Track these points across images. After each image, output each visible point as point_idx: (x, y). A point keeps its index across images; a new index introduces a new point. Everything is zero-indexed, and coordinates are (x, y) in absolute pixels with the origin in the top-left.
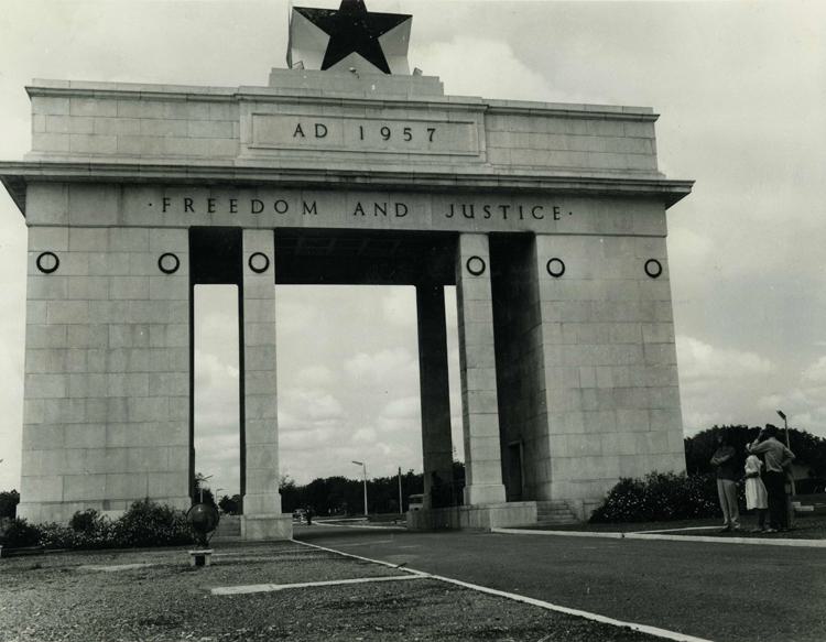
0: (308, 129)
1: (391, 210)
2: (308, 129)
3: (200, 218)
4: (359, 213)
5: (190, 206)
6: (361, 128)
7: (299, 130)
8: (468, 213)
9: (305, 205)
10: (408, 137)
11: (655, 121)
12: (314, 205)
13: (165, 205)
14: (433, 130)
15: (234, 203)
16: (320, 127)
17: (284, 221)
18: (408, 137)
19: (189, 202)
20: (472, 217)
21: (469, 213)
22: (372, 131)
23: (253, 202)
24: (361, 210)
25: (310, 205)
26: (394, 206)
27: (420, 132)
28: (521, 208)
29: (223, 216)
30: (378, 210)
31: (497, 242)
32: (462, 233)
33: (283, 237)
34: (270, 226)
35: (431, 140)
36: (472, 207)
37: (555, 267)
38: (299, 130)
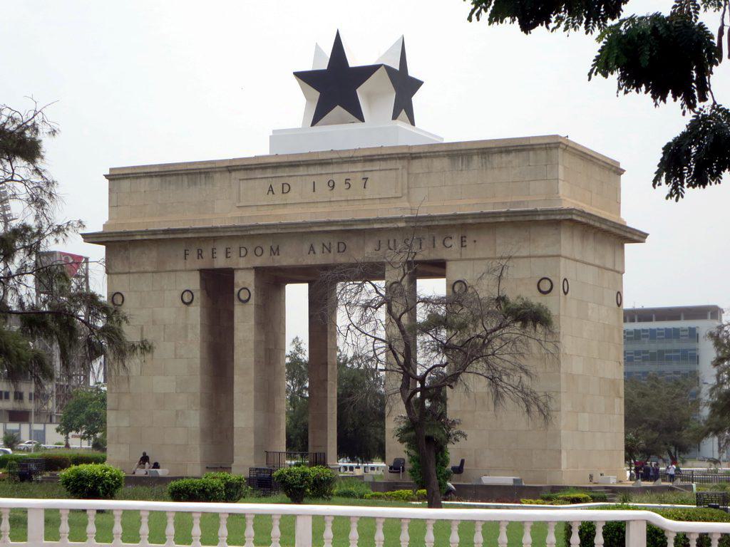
0: (278, 188)
1: (335, 248)
2: (278, 188)
4: (312, 252)
5: (201, 254)
7: (271, 189)
10: (347, 186)
13: (185, 254)
17: (259, 262)
18: (347, 186)
19: (200, 252)
22: (322, 183)
24: (313, 250)
25: (275, 249)
27: (357, 182)
29: (221, 262)
30: (325, 248)
34: (249, 266)
35: (365, 187)
36: (395, 240)
38: (271, 189)
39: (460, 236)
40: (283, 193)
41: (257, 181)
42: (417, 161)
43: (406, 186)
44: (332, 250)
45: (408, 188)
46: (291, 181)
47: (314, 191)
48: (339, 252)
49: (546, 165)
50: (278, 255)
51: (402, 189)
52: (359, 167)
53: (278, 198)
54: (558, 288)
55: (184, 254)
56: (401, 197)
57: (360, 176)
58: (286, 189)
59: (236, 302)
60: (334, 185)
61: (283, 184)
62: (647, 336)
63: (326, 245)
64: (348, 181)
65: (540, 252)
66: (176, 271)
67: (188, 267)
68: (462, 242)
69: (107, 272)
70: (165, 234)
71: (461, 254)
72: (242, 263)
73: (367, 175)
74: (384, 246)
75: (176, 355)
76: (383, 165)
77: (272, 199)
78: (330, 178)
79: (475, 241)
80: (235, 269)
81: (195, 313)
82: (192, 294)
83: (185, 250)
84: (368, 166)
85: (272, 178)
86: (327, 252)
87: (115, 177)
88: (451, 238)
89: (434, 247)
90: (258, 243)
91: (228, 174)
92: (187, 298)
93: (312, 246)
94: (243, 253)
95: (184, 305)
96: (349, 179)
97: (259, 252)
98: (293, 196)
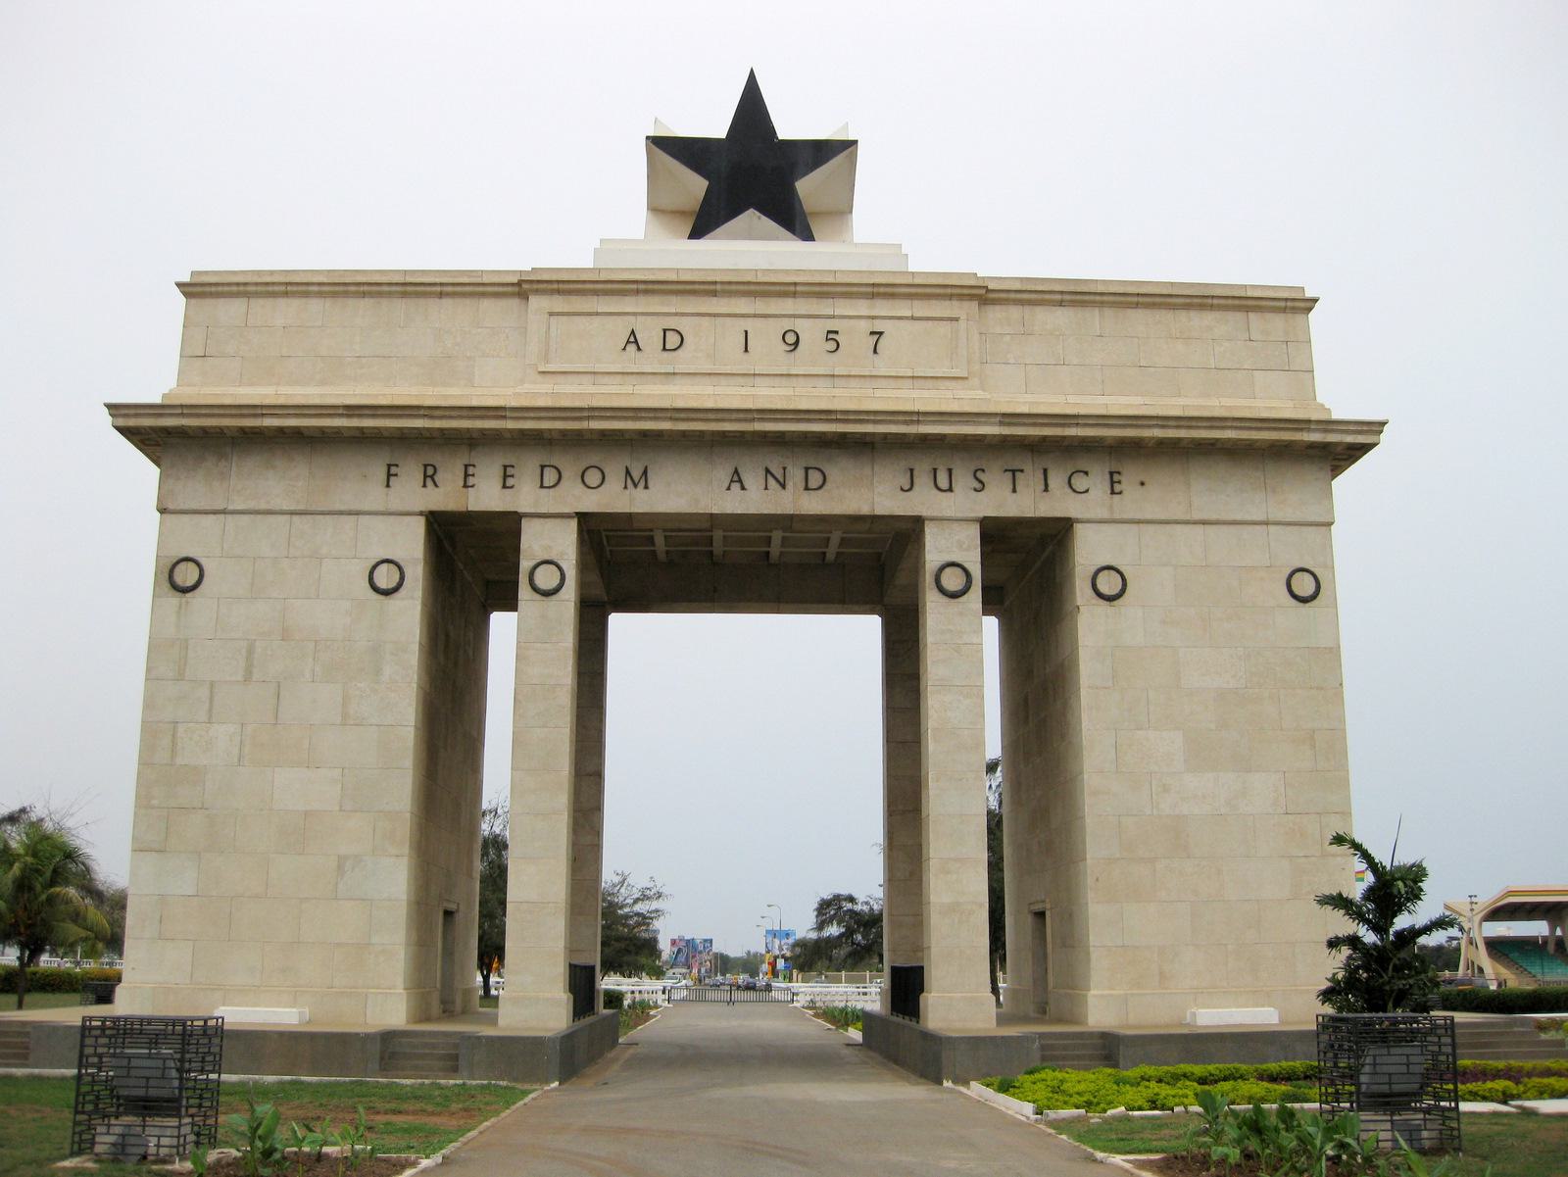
0: (650, 336)
1: (796, 476)
2: (650, 336)
3: (446, 497)
5: (432, 477)
6: (746, 332)
7: (633, 339)
8: (943, 482)
9: (628, 472)
10: (832, 346)
11: (1311, 309)
12: (645, 472)
13: (389, 475)
14: (881, 333)
15: (393, 470)
17: (593, 502)
18: (832, 346)
19: (430, 471)
20: (950, 489)
21: (943, 482)
22: (767, 337)
23: (543, 467)
24: (740, 481)
25: (636, 474)
26: (802, 473)
27: (855, 336)
28: (1045, 471)
29: (486, 496)
30: (770, 479)
31: (996, 535)
32: (1078, 521)
33: (594, 531)
34: (567, 510)
35: (875, 351)
36: (950, 471)
37: (1108, 584)
38: (633, 339)
39: (1107, 470)
40: (664, 349)
41: (597, 320)
42: (998, 307)
44: (790, 485)
46: (684, 325)
47: (746, 350)
48: (807, 488)
50: (646, 487)
52: (862, 307)
53: (651, 359)
56: (966, 378)
57: (865, 326)
58: (672, 341)
61: (665, 331)
64: (831, 336)
65: (1289, 514)
66: (358, 513)
67: (395, 504)
70: (349, 416)
71: (1111, 508)
72: (548, 502)
73: (878, 326)
75: (345, 716)
76: (921, 308)
77: (631, 361)
78: (787, 324)
79: (1142, 484)
81: (408, 614)
82: (400, 568)
83: (389, 466)
84: (882, 308)
85: (635, 314)
86: (778, 486)
87: (195, 290)
88: (1086, 473)
89: (1046, 489)
90: (594, 459)
91: (515, 302)
92: (385, 577)
93: (736, 471)
94: (550, 477)
96: (836, 332)
98: (683, 361)
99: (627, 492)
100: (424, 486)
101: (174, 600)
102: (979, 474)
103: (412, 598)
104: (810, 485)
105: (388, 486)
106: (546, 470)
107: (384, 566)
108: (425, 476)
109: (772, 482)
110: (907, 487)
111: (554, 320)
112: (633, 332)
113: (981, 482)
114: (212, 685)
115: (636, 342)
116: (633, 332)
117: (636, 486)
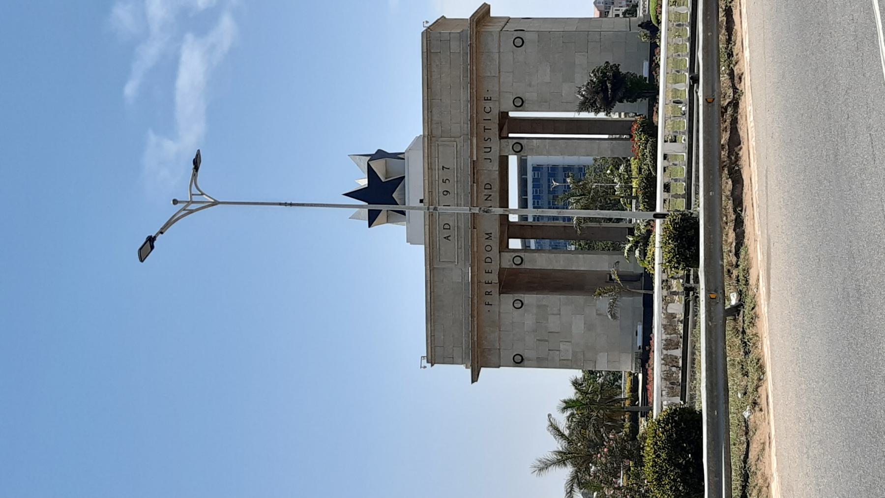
8: (489, 150)
10: (447, 181)
12: (487, 234)
13: (488, 304)
14: (443, 167)
16: (445, 228)
18: (447, 181)
20: (490, 148)
21: (489, 150)
25: (487, 236)
29: (494, 278)
34: (498, 256)
35: (449, 169)
39: (484, 101)
43: (450, 139)
45: (451, 137)
49: (441, 40)
50: (491, 234)
51: (451, 141)
54: (519, 34)
55: (488, 306)
59: (523, 266)
60: (447, 191)
61: (444, 229)
62: (538, 202)
63: (485, 198)
64: (444, 181)
67: (497, 303)
68: (487, 100)
69: (499, 367)
74: (488, 156)
79: (488, 91)
80: (500, 267)
81: (530, 299)
85: (439, 237)
88: (485, 108)
95: (523, 307)
96: (443, 180)
97: (488, 248)
99: (493, 239)
100: (491, 295)
101: (525, 362)
102: (486, 139)
103: (524, 297)
104: (490, 187)
105: (491, 305)
106: (487, 261)
107: (515, 305)
108: (489, 294)
109: (489, 199)
110: (490, 161)
111: (441, 260)
112: (445, 238)
113: (488, 139)
114: (549, 350)
115: (448, 237)
116: (445, 238)
117: (491, 237)
